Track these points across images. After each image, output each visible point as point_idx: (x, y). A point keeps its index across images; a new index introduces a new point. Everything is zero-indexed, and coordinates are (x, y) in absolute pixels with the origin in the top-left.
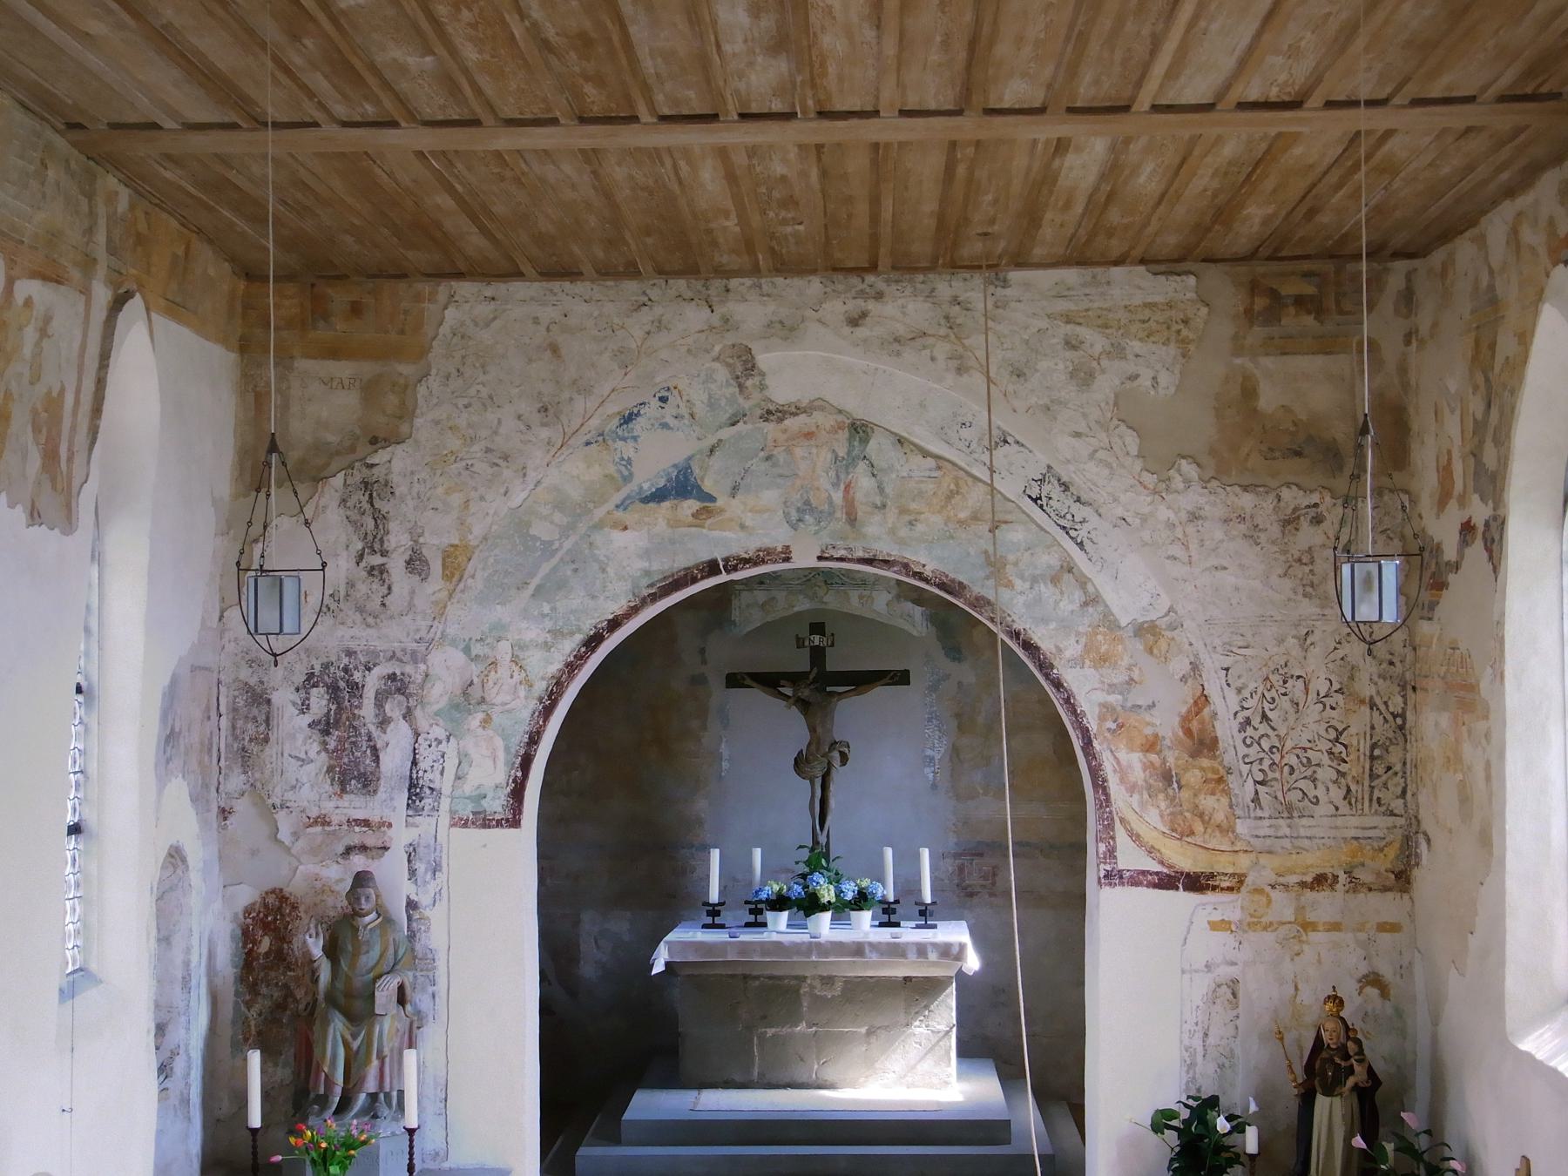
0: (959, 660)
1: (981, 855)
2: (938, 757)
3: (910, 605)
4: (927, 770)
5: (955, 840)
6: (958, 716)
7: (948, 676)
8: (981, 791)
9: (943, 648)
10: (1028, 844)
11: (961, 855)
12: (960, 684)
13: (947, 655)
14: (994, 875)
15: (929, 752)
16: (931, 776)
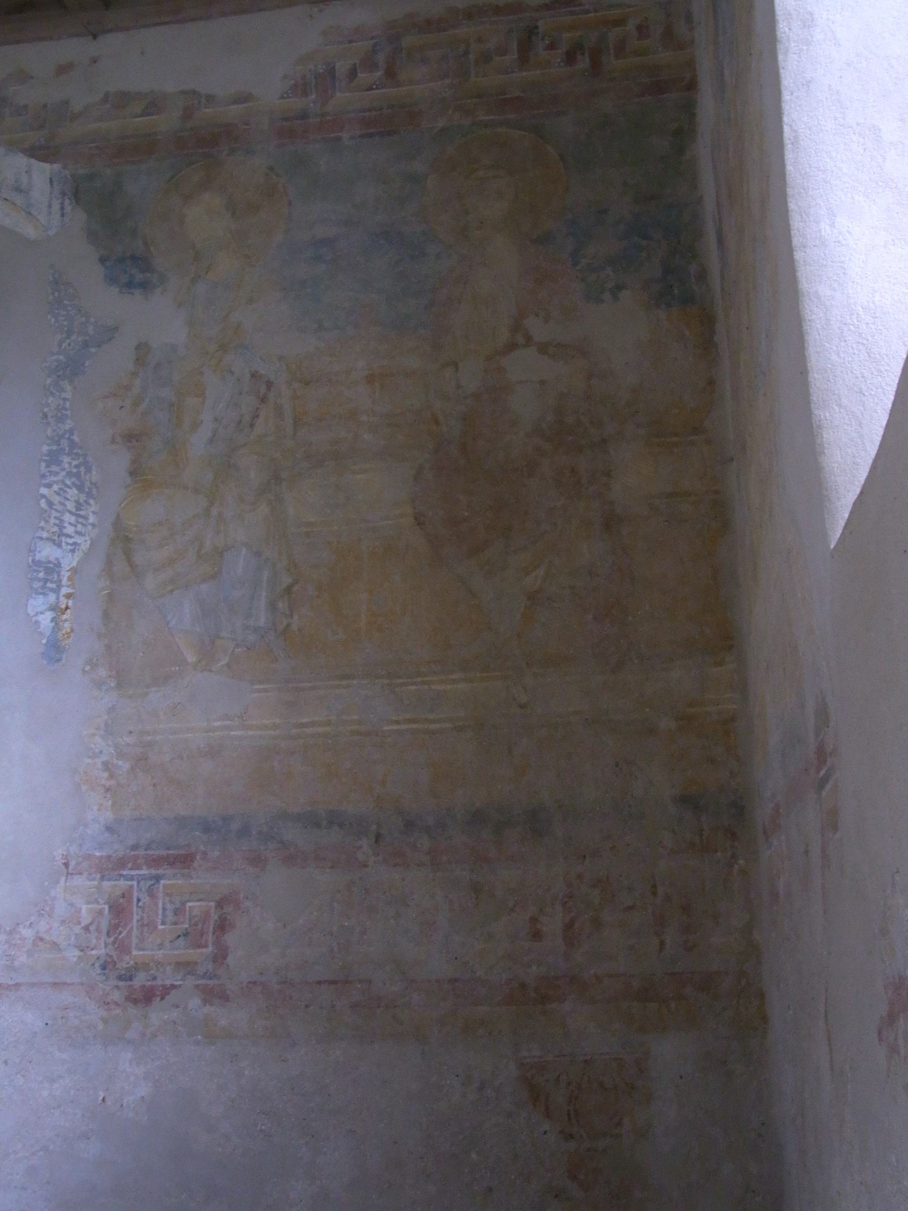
0: (145, 287)
1: (184, 861)
2: (69, 562)
3: (21, 161)
4: (38, 603)
5: (109, 815)
6: (132, 438)
7: (110, 333)
8: (191, 658)
9: (102, 260)
10: (335, 819)
11: (121, 863)
12: (142, 351)
13: (111, 279)
14: (222, 926)
15: (47, 552)
16: (46, 620)
